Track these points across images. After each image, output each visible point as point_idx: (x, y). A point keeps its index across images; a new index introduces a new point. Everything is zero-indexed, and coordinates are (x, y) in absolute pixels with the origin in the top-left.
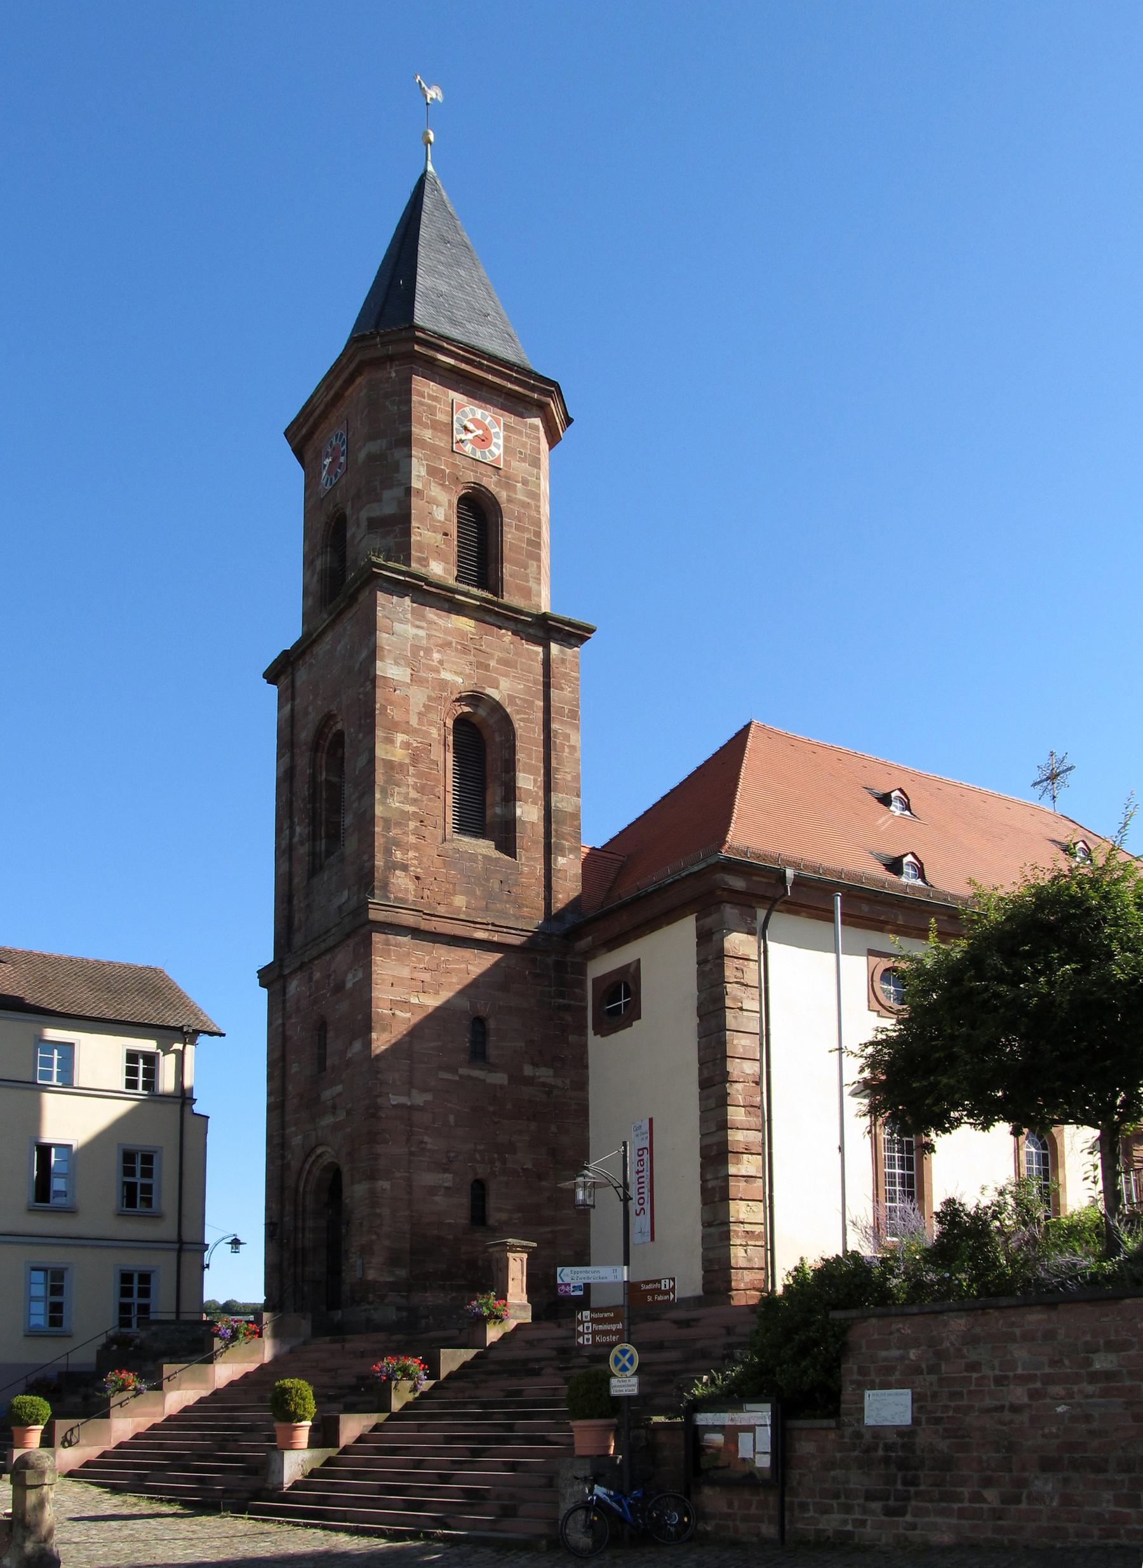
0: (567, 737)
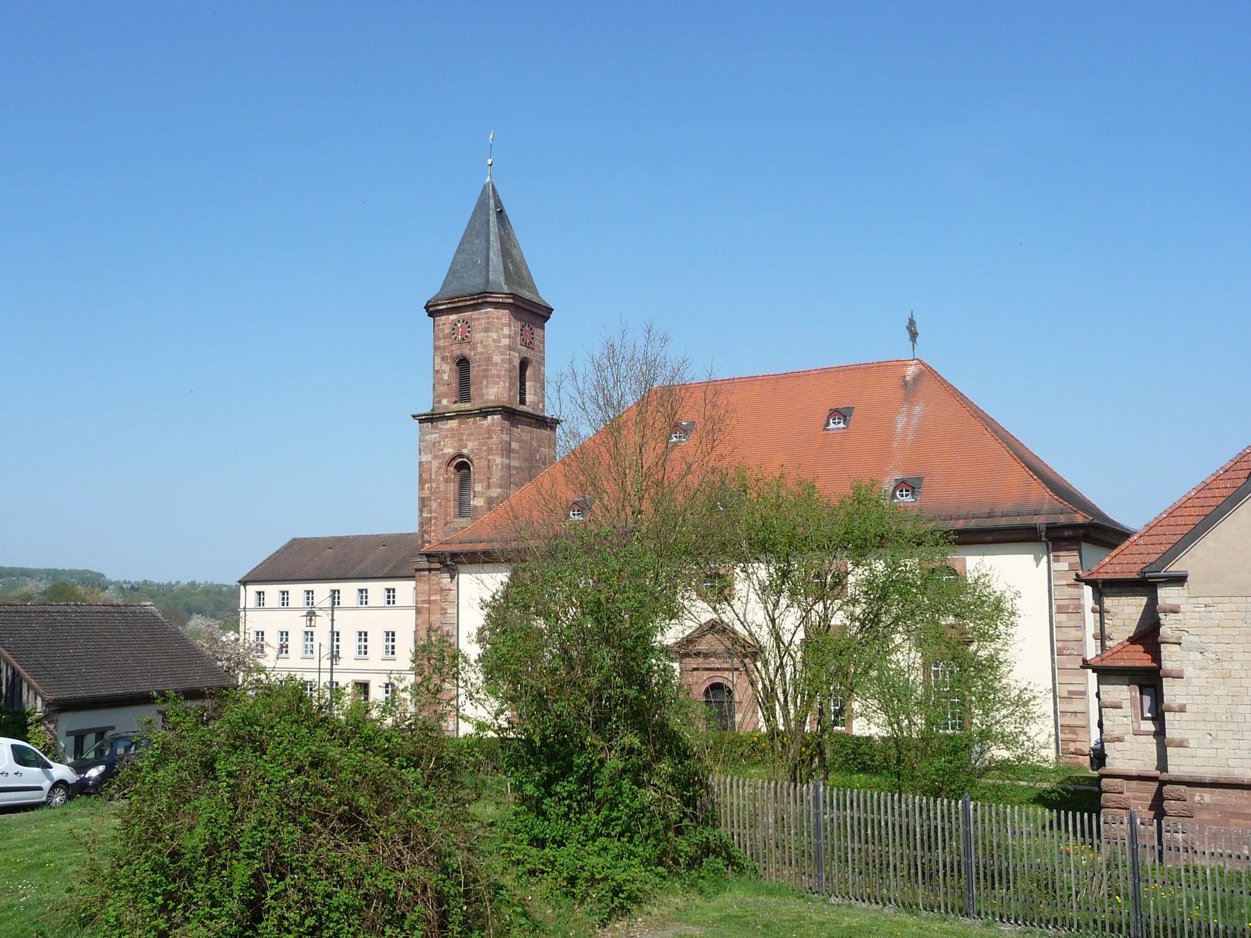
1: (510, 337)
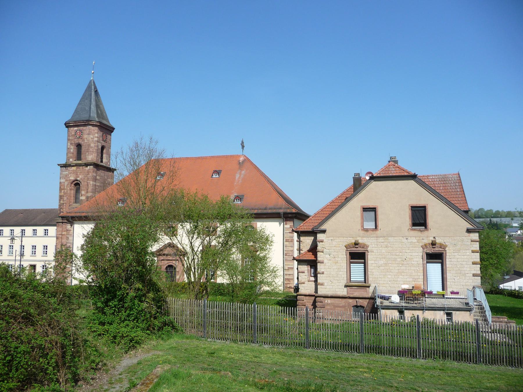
0: (90, 183)
1: (98, 137)
